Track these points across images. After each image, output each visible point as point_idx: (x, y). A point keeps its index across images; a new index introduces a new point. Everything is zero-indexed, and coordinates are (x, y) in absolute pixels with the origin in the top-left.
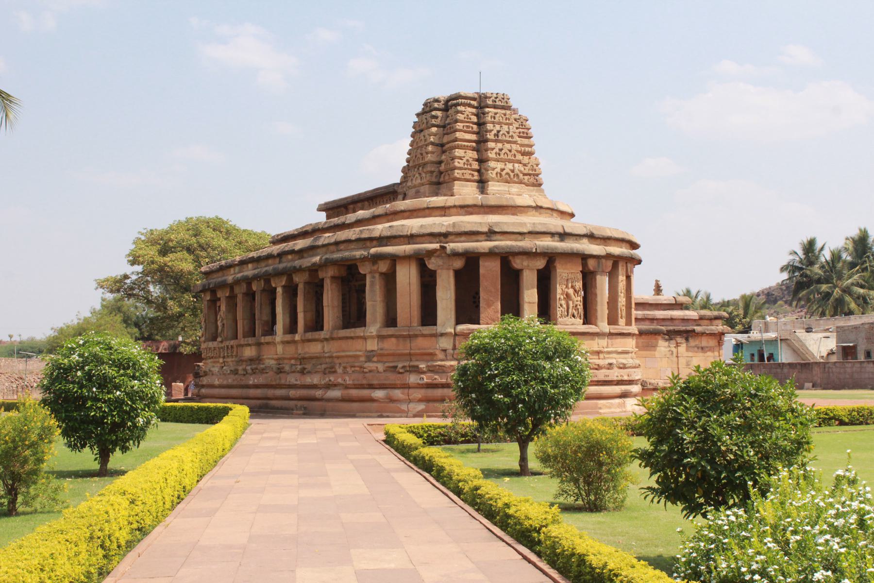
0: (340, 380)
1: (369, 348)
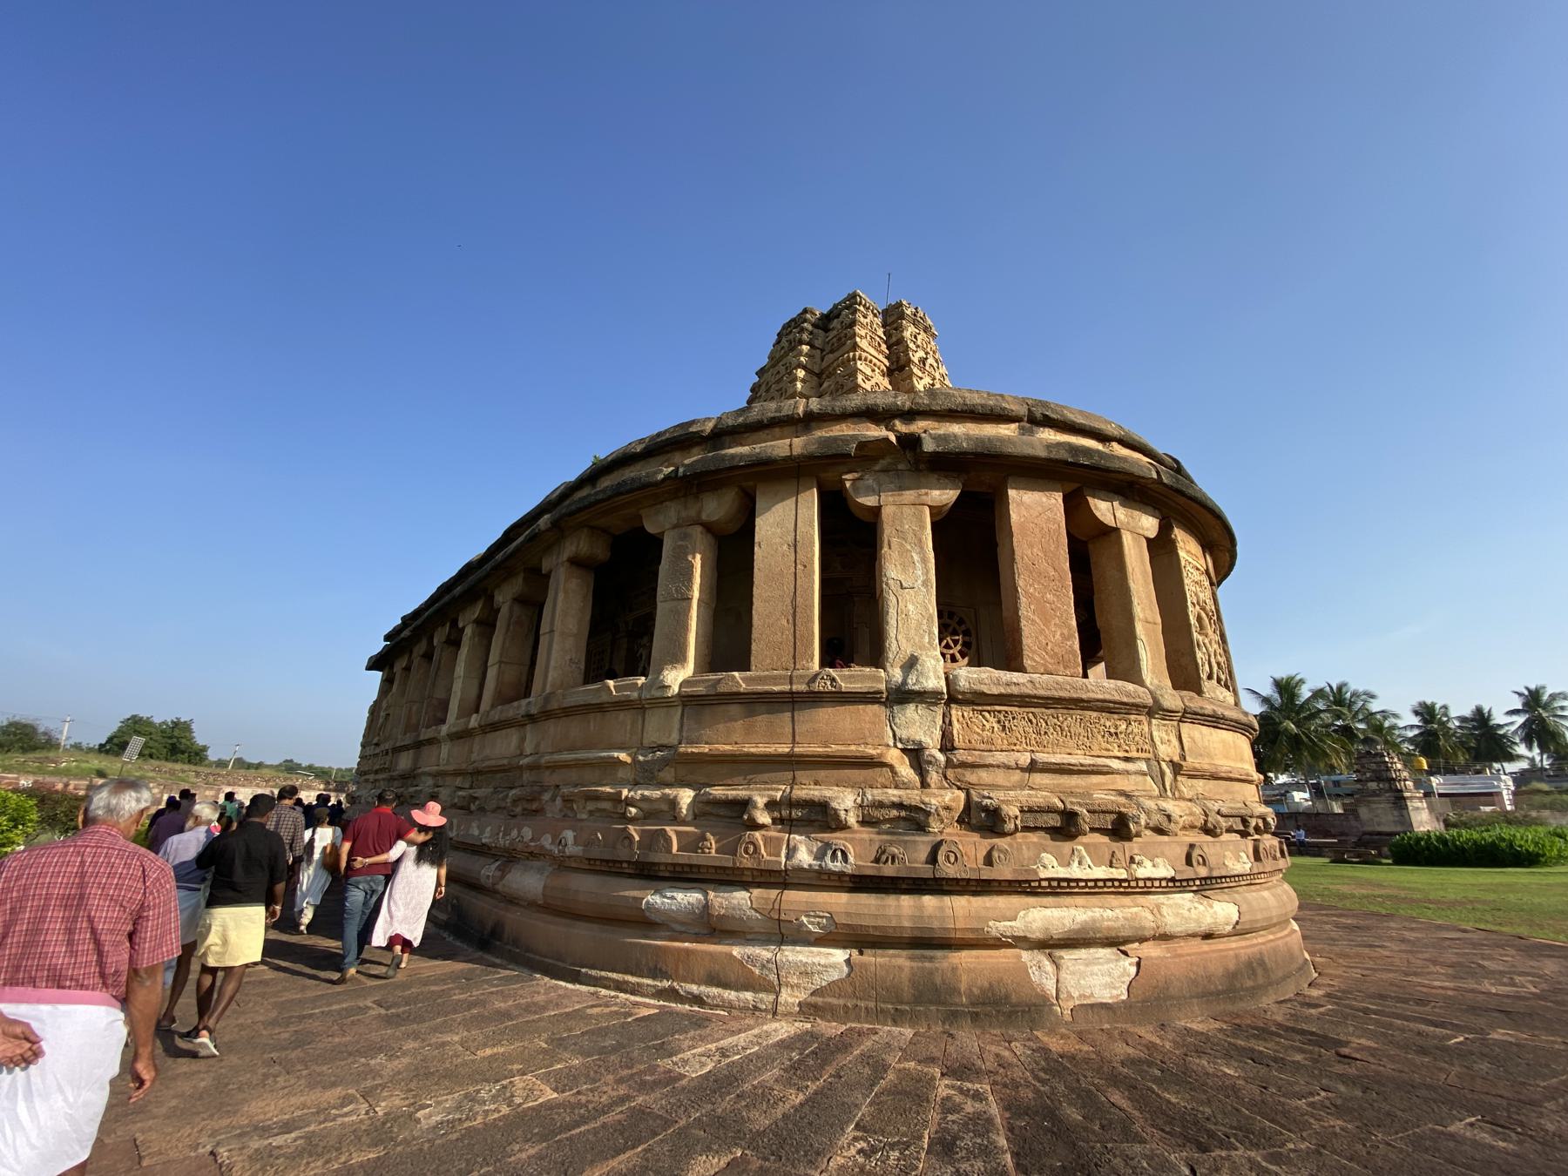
1: (652, 735)
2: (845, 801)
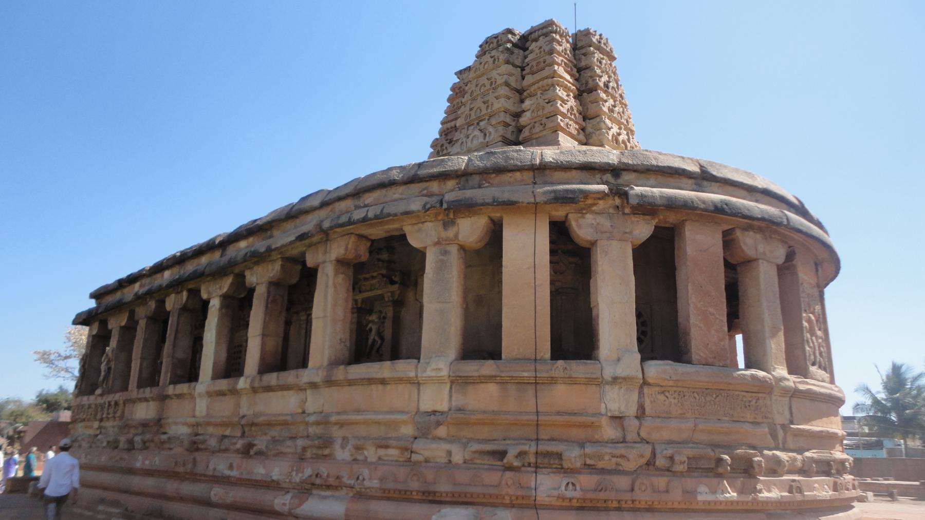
1: (427, 404)
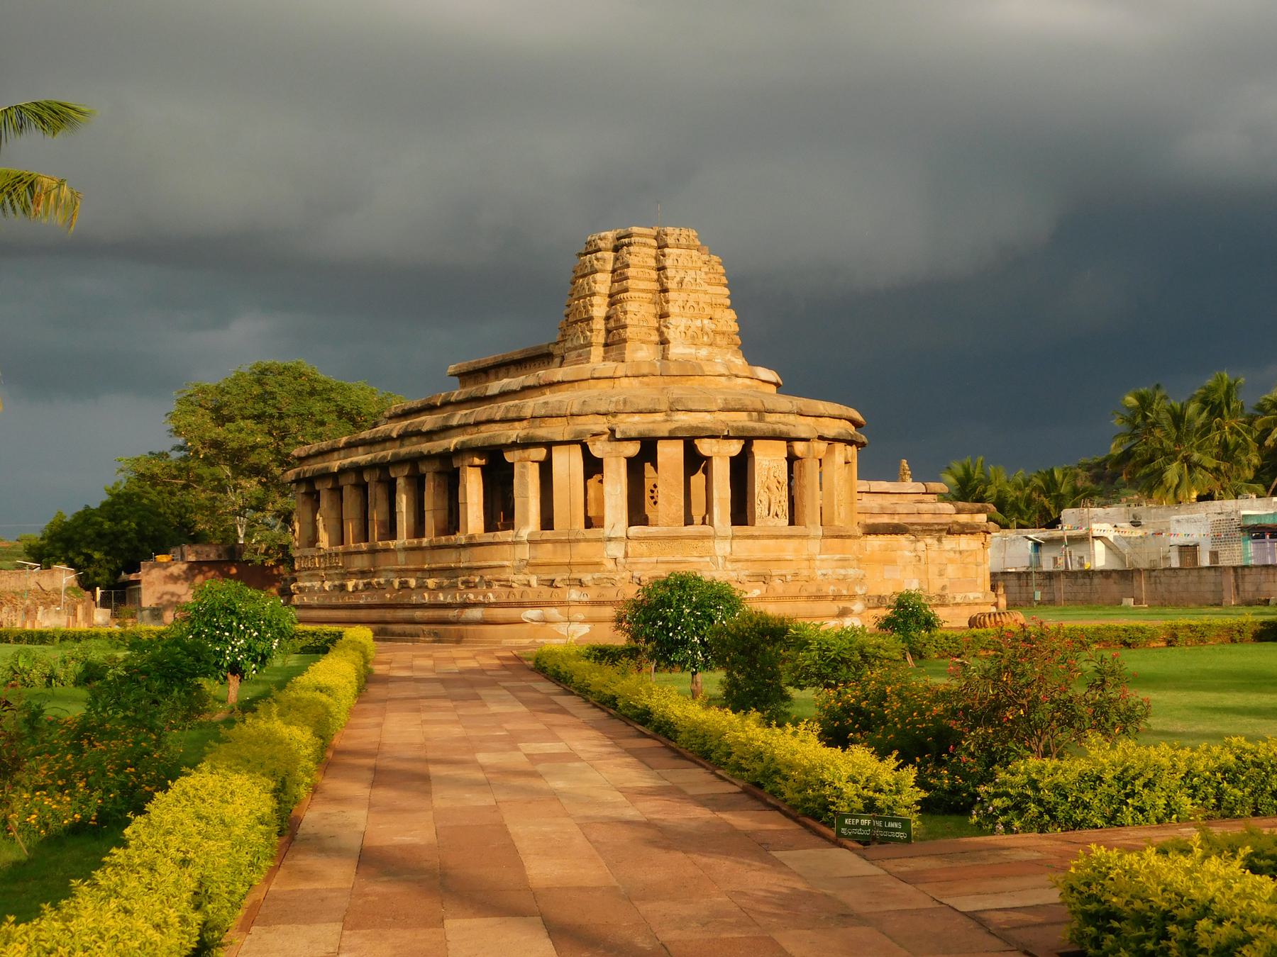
0: (481, 598)
2: (587, 578)
